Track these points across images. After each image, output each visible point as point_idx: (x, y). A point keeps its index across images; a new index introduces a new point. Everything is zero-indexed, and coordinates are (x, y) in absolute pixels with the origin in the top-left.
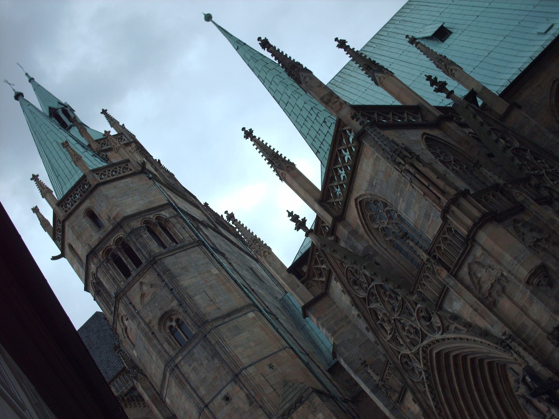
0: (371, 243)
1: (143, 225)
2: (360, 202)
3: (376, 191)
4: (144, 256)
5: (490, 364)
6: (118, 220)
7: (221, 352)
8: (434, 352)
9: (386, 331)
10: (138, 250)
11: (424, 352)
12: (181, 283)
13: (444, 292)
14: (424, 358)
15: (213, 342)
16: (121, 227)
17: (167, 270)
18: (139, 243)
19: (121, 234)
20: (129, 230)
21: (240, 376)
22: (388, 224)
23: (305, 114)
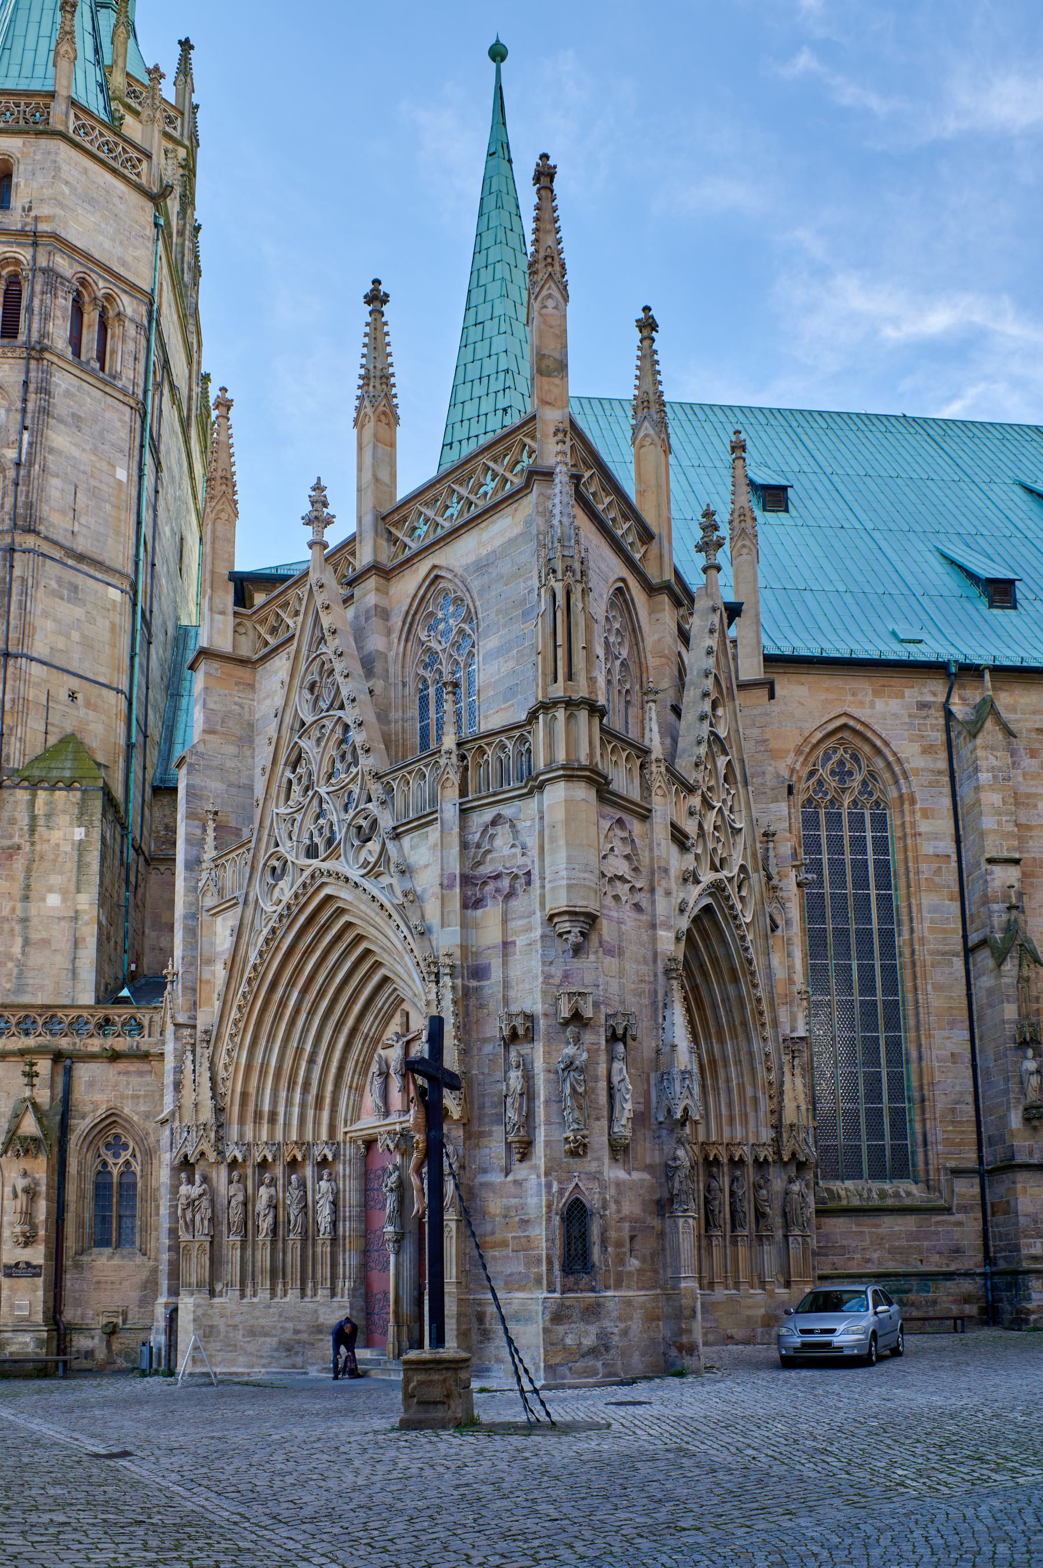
0: (392, 654)
1: (74, 281)
2: (437, 577)
3: (475, 585)
4: (29, 330)
5: (386, 979)
6: (43, 227)
7: (14, 598)
8: (327, 891)
9: (288, 798)
10: (30, 309)
11: (313, 877)
12: (50, 432)
13: (424, 821)
14: (304, 885)
15: (17, 572)
16: (35, 244)
17: (45, 390)
18: (42, 301)
19: (25, 255)
20: (42, 262)
21: (11, 662)
22: (444, 650)
23: (489, 367)
